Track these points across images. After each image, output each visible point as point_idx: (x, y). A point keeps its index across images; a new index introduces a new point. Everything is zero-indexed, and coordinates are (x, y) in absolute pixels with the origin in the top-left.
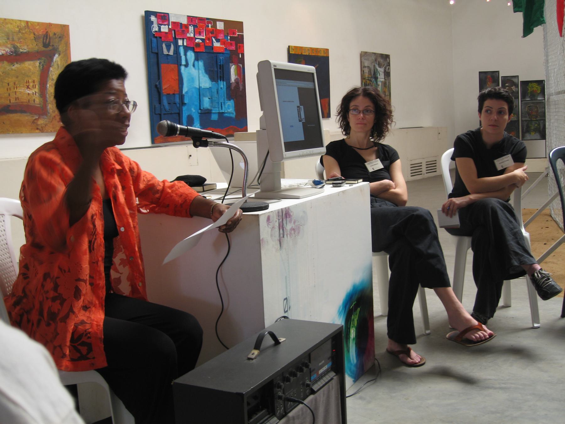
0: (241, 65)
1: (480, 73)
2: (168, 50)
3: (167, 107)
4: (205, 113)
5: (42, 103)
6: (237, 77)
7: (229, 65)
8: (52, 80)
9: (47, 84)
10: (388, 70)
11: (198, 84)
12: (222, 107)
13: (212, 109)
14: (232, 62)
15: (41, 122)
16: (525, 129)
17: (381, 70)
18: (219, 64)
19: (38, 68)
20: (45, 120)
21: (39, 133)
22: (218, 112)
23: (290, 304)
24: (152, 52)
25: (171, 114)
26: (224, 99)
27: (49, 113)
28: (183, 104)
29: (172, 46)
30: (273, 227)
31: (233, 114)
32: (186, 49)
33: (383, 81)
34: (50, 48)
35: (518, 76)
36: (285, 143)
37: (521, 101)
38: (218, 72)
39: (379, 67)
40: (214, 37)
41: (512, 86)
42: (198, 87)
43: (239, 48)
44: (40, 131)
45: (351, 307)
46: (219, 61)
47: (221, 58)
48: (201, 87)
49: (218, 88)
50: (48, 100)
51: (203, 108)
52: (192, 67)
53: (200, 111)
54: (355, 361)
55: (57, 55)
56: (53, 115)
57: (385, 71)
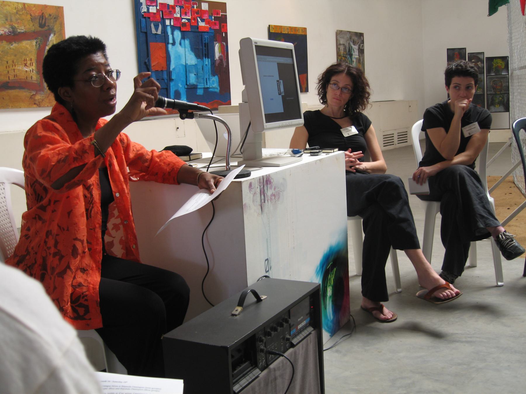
1: (448, 49)
5: (39, 80)
6: (220, 54)
10: (362, 47)
11: (184, 61)
12: (207, 82)
13: (198, 84)
14: (216, 41)
15: (38, 97)
16: (490, 102)
17: (355, 48)
18: (204, 42)
19: (35, 47)
20: (42, 95)
22: (203, 87)
23: (271, 265)
26: (209, 75)
28: (170, 79)
30: (255, 193)
31: (217, 89)
33: (358, 58)
35: (484, 52)
37: (487, 76)
38: (203, 49)
39: (354, 45)
41: (478, 62)
42: (184, 64)
44: (37, 105)
46: (204, 40)
47: (206, 37)
48: (188, 64)
49: (203, 65)
51: (190, 84)
52: (179, 45)
53: (186, 87)
54: (332, 317)
55: (52, 35)
57: (359, 48)
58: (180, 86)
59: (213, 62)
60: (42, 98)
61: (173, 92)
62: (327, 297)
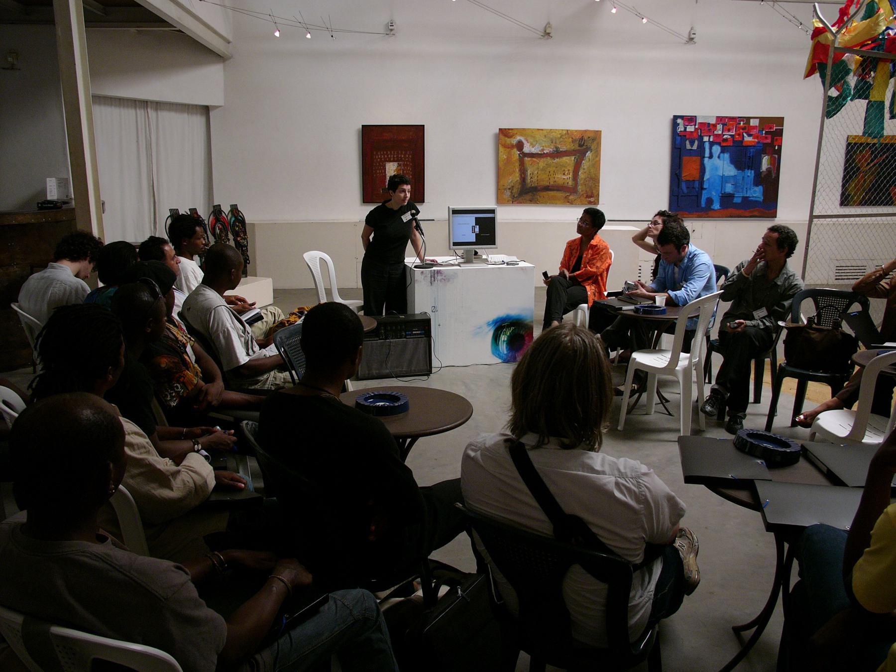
0: (776, 156)
2: (692, 145)
4: (726, 197)
5: (574, 185)
6: (769, 166)
7: (761, 156)
12: (747, 192)
13: (735, 193)
15: (571, 197)
19: (573, 161)
24: (676, 148)
28: (702, 189)
29: (696, 143)
32: (711, 144)
34: (584, 147)
36: (453, 243)
40: (746, 133)
42: (722, 175)
43: (776, 141)
44: (570, 203)
47: (752, 150)
51: (725, 193)
52: (717, 158)
53: (720, 195)
54: (505, 352)
55: (589, 152)
56: (582, 193)
58: (714, 193)
59: (758, 174)
61: (705, 199)
62: (500, 341)
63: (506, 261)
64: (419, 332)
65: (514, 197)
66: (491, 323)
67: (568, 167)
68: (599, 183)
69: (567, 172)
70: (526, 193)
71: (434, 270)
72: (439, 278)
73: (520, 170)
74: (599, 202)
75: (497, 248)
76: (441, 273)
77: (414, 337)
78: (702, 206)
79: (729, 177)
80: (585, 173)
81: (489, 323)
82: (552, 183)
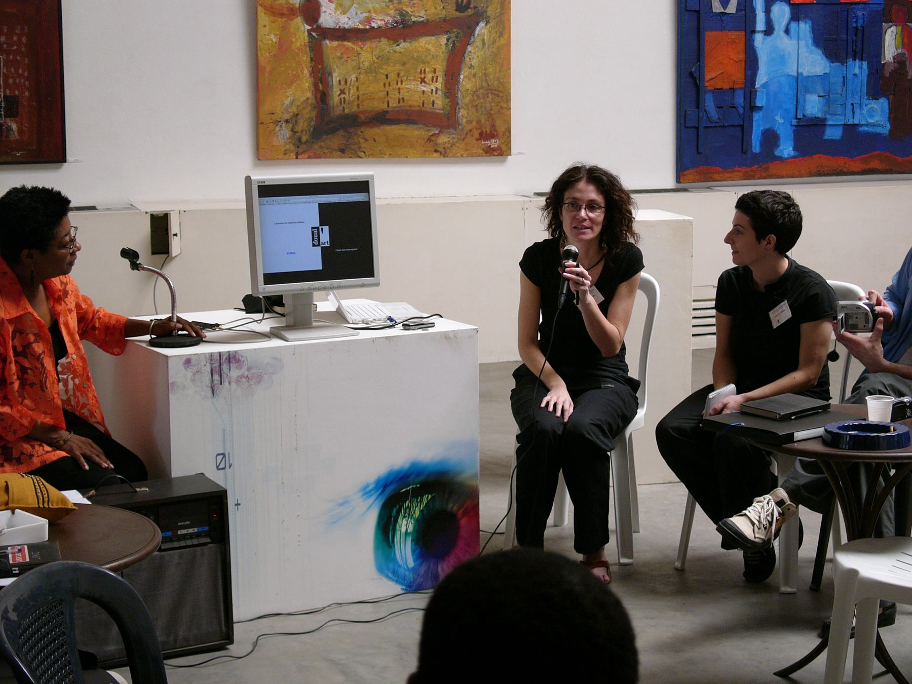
3: (714, 113)
5: (448, 108)
8: (470, 68)
9: (459, 75)
11: (795, 69)
13: (828, 117)
15: (443, 139)
20: (452, 136)
21: (440, 157)
22: (843, 123)
25: (723, 127)
27: (459, 124)
28: (753, 108)
30: (197, 372)
36: (265, 275)
42: (796, 75)
44: (441, 154)
45: (402, 489)
48: (802, 74)
50: (460, 102)
51: (804, 116)
53: (794, 122)
54: (411, 563)
56: (469, 127)
60: (451, 142)
62: (398, 533)
63: (399, 316)
64: (196, 530)
65: (300, 140)
66: (371, 487)
67: (432, 62)
68: (508, 100)
69: (429, 76)
70: (334, 131)
71: (220, 354)
72: (234, 373)
73: (313, 73)
74: (510, 149)
75: (378, 285)
76: (238, 361)
77: (183, 544)
78: (754, 151)
79: (811, 78)
80: (474, 76)
81: (368, 486)
82: (393, 104)
